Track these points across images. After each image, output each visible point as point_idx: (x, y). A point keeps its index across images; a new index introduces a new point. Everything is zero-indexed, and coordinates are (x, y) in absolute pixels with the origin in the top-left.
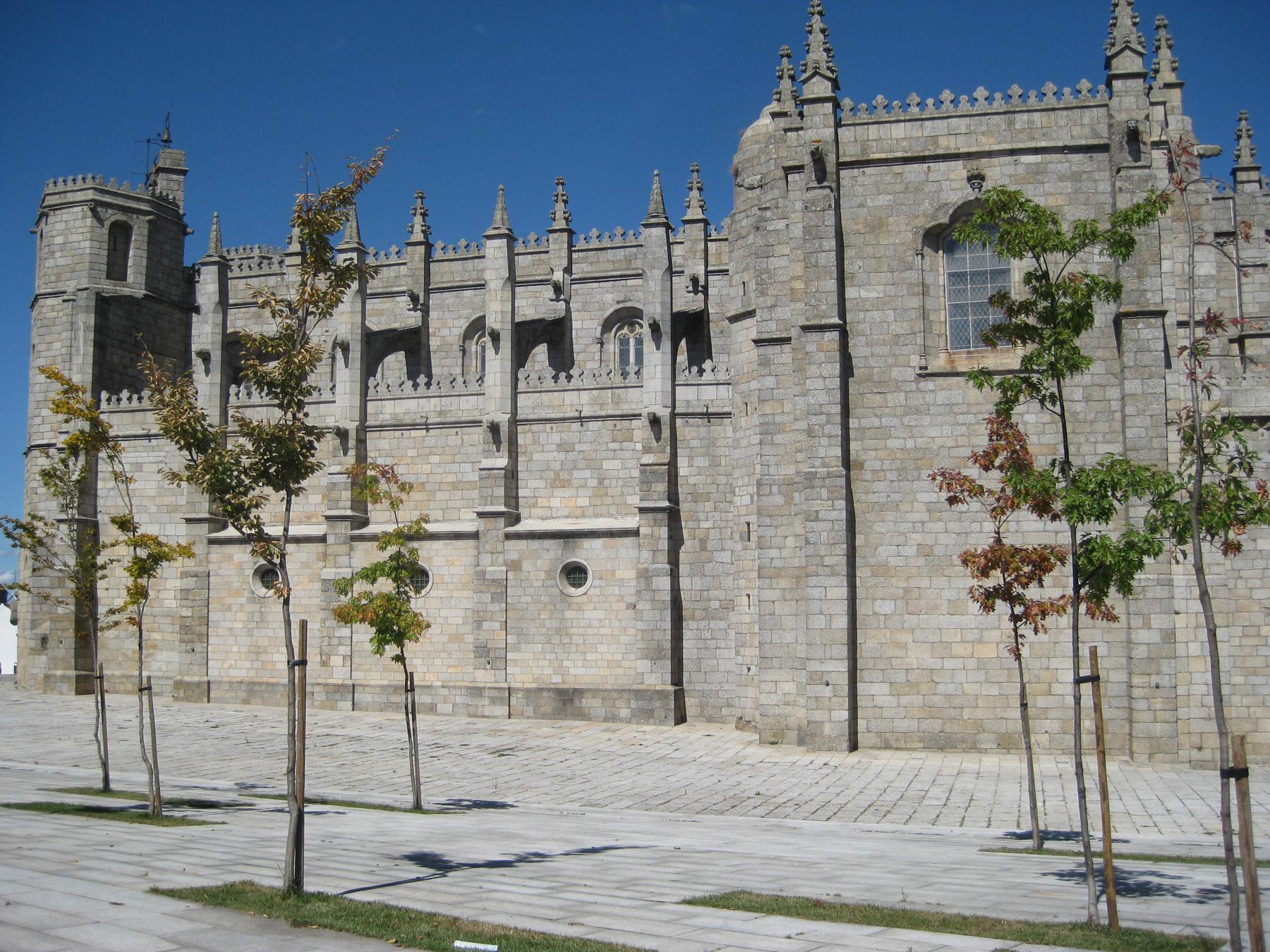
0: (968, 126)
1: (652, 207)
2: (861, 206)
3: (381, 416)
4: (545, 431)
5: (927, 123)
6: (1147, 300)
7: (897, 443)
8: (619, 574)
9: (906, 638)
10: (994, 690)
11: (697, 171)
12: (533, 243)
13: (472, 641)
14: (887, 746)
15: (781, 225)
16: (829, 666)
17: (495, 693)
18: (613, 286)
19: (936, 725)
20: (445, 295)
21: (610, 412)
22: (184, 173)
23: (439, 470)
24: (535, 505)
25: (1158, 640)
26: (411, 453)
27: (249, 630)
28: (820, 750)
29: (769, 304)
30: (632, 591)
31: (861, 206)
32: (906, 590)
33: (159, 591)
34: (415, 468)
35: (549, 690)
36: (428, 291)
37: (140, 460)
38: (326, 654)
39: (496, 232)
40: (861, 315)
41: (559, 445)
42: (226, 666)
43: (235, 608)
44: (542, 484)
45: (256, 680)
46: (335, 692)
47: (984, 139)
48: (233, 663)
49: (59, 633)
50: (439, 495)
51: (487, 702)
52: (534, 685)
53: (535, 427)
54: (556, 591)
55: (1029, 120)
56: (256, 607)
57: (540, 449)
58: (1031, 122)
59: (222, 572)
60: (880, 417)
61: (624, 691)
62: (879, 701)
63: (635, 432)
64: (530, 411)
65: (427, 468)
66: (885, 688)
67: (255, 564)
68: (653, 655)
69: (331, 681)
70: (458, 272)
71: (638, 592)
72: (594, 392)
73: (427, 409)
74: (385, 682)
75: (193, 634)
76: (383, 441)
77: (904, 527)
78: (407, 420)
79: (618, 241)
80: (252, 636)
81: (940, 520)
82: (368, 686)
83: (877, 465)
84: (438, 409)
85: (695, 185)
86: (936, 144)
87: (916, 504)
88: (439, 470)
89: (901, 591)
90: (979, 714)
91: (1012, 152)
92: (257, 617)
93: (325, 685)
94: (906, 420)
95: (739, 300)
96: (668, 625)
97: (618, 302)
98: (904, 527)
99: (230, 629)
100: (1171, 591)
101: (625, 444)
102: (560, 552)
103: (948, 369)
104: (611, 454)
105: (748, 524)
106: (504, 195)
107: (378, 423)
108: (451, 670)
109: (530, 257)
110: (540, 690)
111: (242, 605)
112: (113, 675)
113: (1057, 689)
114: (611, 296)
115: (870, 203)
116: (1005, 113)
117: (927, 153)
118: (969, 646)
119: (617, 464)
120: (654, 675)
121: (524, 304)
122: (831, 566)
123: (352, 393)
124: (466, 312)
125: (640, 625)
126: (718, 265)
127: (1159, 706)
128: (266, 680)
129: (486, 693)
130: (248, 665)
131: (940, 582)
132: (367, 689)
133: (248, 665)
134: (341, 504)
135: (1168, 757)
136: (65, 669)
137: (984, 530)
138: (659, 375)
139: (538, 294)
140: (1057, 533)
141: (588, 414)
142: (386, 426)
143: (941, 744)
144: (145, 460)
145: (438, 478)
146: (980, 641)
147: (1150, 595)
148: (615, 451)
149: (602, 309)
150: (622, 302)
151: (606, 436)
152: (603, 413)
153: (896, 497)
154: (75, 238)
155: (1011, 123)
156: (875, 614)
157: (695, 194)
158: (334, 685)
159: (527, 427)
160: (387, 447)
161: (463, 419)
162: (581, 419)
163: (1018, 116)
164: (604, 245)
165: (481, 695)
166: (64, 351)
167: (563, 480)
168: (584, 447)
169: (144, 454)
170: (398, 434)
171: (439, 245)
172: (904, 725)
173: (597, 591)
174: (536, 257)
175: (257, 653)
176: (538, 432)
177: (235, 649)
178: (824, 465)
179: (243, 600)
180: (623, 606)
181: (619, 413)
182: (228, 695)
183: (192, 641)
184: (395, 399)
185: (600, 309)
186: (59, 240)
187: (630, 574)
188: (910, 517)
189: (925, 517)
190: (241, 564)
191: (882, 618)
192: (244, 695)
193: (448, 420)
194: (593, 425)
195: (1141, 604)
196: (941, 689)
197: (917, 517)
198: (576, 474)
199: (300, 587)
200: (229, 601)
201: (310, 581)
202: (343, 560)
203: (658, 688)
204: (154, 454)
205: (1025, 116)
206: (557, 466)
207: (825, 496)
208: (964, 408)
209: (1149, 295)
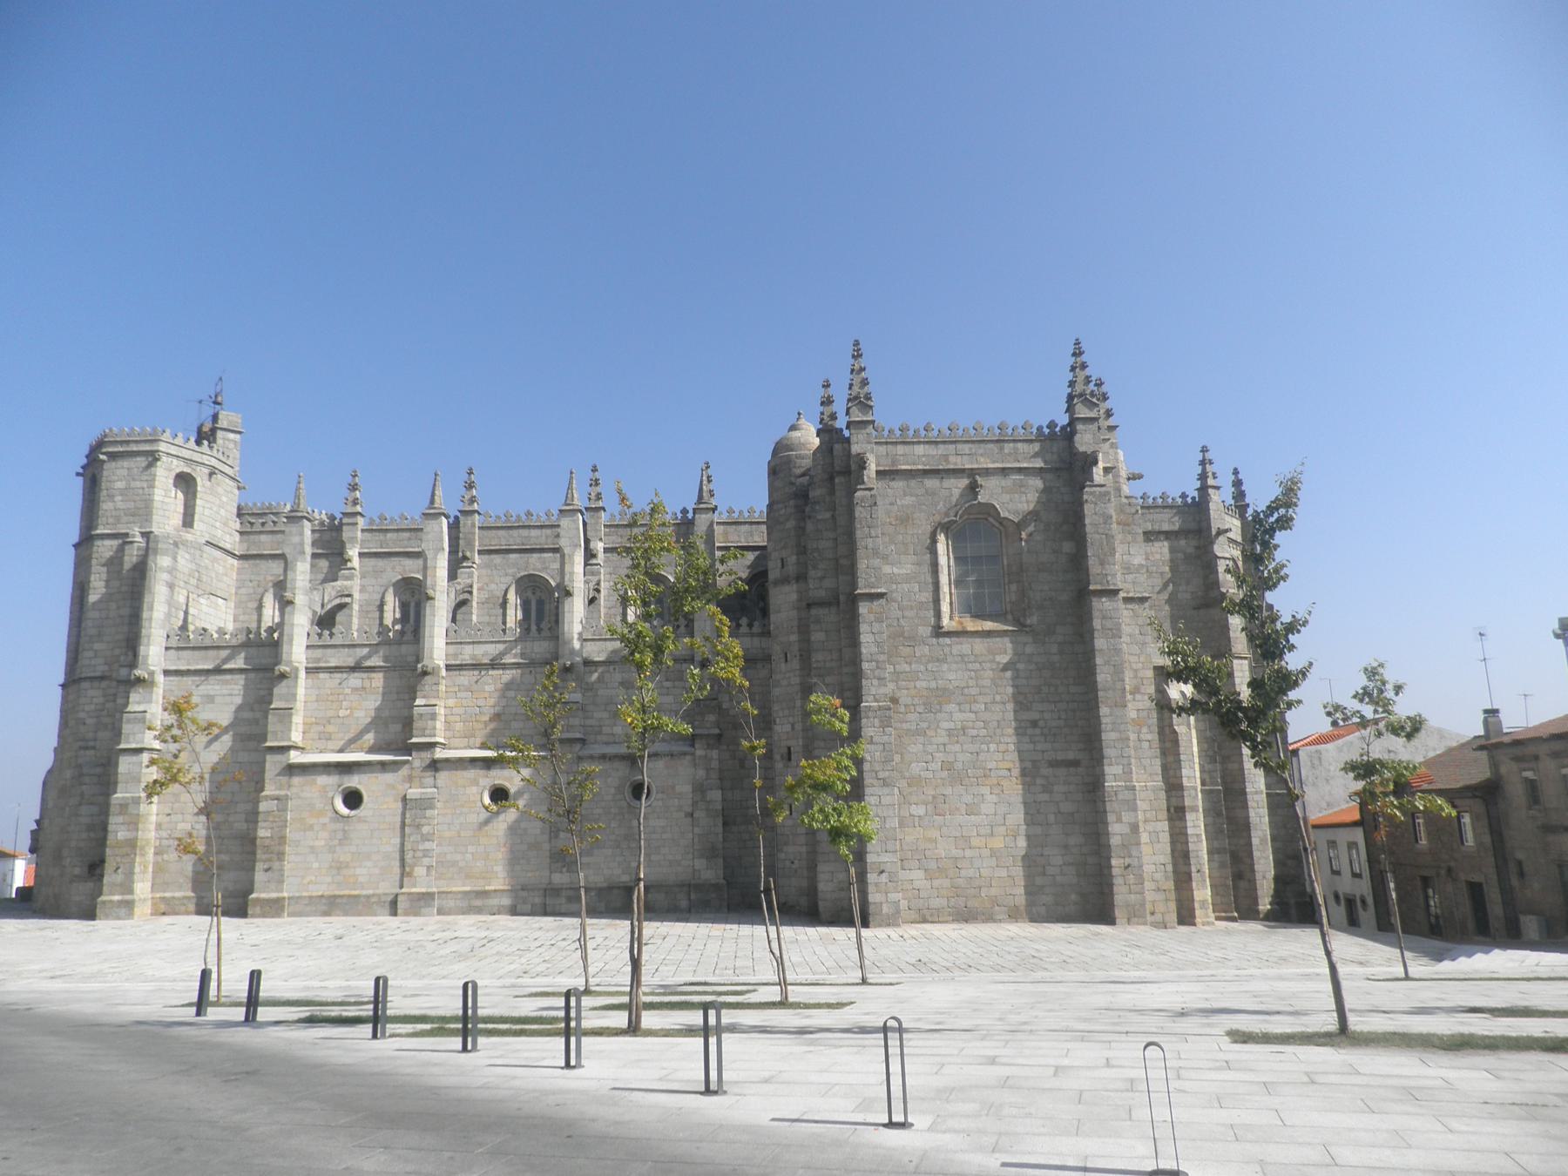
0: (970, 449)
2: (891, 504)
4: (608, 671)
5: (941, 446)
6: (1108, 582)
7: (924, 684)
8: (678, 789)
9: (934, 834)
10: (1004, 873)
13: (548, 848)
14: (925, 921)
15: (828, 515)
16: (885, 858)
17: (571, 893)
19: (961, 902)
20: (493, 556)
22: (240, 433)
24: (600, 733)
25: (1128, 831)
27: (330, 847)
28: (880, 926)
29: (819, 575)
30: (690, 802)
31: (891, 504)
32: (934, 797)
33: (228, 814)
35: (619, 888)
37: (212, 693)
38: (410, 866)
39: (571, 507)
40: (894, 586)
41: (622, 684)
42: (305, 881)
43: (316, 828)
44: (605, 715)
45: (337, 893)
46: (419, 900)
47: (982, 460)
48: (313, 878)
49: (118, 859)
50: (514, 725)
51: (563, 900)
52: (605, 885)
54: (625, 804)
55: (1014, 448)
56: (339, 826)
58: (1016, 449)
59: (304, 795)
60: (910, 664)
61: (684, 885)
62: (917, 884)
66: (920, 874)
67: (339, 786)
68: (710, 853)
69: (414, 890)
70: (504, 537)
71: (694, 804)
74: (468, 889)
75: (272, 853)
77: (930, 749)
80: (334, 852)
81: (957, 742)
82: (450, 892)
83: (909, 701)
86: (947, 461)
87: (939, 731)
89: (930, 798)
90: (993, 891)
91: (1004, 471)
92: (340, 835)
93: (410, 894)
94: (930, 666)
95: (778, 570)
96: (720, 829)
98: (930, 749)
99: (312, 847)
100: (1135, 795)
101: (676, 683)
102: (627, 772)
103: (960, 629)
105: (789, 748)
107: (458, 662)
108: (530, 874)
110: (610, 888)
111: (325, 824)
112: (173, 898)
113: (1050, 870)
115: (899, 502)
116: (998, 441)
117: (941, 467)
118: (983, 839)
120: (709, 871)
122: (884, 779)
124: (510, 571)
125: (697, 830)
127: (1131, 882)
128: (347, 892)
129: (564, 893)
130: (329, 879)
131: (960, 789)
132: (450, 896)
133: (329, 879)
134: (427, 732)
135: (1141, 920)
136: (123, 894)
137: (992, 750)
140: (1043, 752)
143: (966, 916)
144: (218, 693)
146: (992, 835)
147: (1120, 797)
153: (925, 725)
154: (138, 484)
155: (1002, 449)
156: (910, 815)
158: (418, 894)
160: (466, 683)
163: (1006, 445)
165: (558, 895)
166: (124, 589)
169: (217, 687)
170: (476, 673)
172: (936, 903)
173: (660, 803)
175: (339, 869)
177: (316, 865)
178: (876, 701)
179: (326, 820)
180: (683, 814)
182: (308, 909)
183: (270, 860)
186: (120, 485)
187: (687, 788)
188: (934, 740)
189: (946, 740)
190: (324, 787)
191: (917, 819)
192: (324, 908)
195: (1115, 805)
196: (963, 873)
197: (941, 740)
199: (385, 806)
200: (312, 821)
201: (396, 801)
202: (429, 781)
203: (713, 882)
204: (229, 687)
205: (1011, 445)
207: (877, 724)
208: (972, 658)
209: (1109, 578)
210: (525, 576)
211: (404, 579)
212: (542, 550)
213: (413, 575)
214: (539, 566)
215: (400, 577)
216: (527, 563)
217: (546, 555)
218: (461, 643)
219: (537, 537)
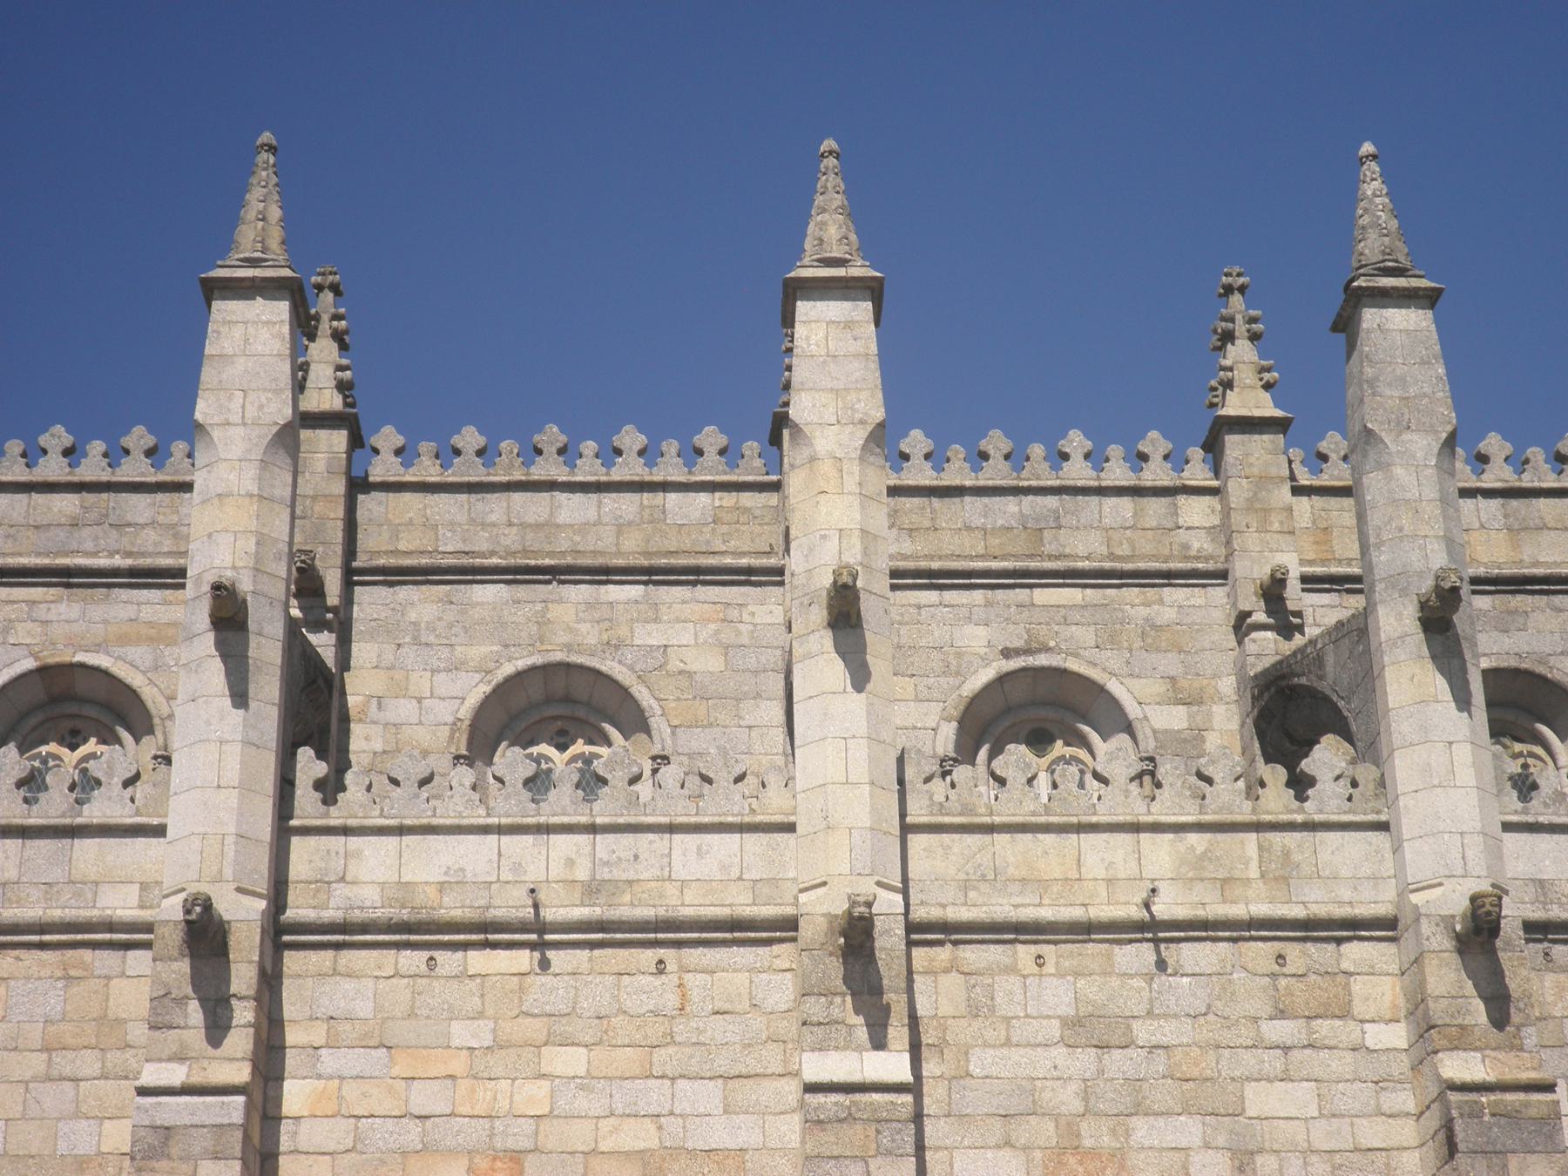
1: (1371, 247)
3: (340, 891)
4: (1012, 969)
11: (1242, 289)
12: (711, 456)
18: (989, 604)
20: (405, 593)
21: (1261, 909)
23: (582, 1103)
26: (461, 1034)
34: (484, 1092)
36: (351, 576)
53: (973, 955)
57: (995, 1034)
63: (1358, 986)
64: (950, 894)
65: (534, 1096)
70: (452, 525)
72: (1193, 838)
73: (534, 873)
76: (348, 985)
78: (453, 908)
79: (996, 473)
84: (582, 874)
85: (1241, 328)
88: (582, 1103)
97: (1007, 653)
101: (1324, 1027)
104: (1273, 1062)
106: (844, 173)
107: (330, 914)
109: (703, 498)
114: (981, 631)
119: (1295, 1099)
121: (687, 638)
123: (245, 788)
124: (478, 652)
126: (1324, 562)
138: (1466, 776)
139: (734, 613)
141: (1182, 913)
142: (365, 928)
145: (579, 1135)
148: (1286, 1049)
149: (955, 669)
150: (1018, 652)
151: (1252, 997)
152: (1237, 911)
157: (1241, 353)
159: (944, 954)
160: (364, 1008)
161: (688, 912)
162: (1150, 929)
164: (950, 478)
167: (1093, 1153)
168: (1168, 1032)
170: (413, 960)
171: (387, 438)
174: (728, 499)
176: (989, 971)
181: (1296, 912)
184: (401, 831)
185: (946, 671)
193: (624, 912)
194: (1194, 955)
198: (1143, 1131)
206: (1068, 1099)
210: (533, 669)
211: (44, 671)
212: (603, 574)
213: (80, 657)
214: (590, 634)
215: (29, 664)
216: (543, 622)
217: (615, 592)
218: (346, 831)
219: (583, 528)
